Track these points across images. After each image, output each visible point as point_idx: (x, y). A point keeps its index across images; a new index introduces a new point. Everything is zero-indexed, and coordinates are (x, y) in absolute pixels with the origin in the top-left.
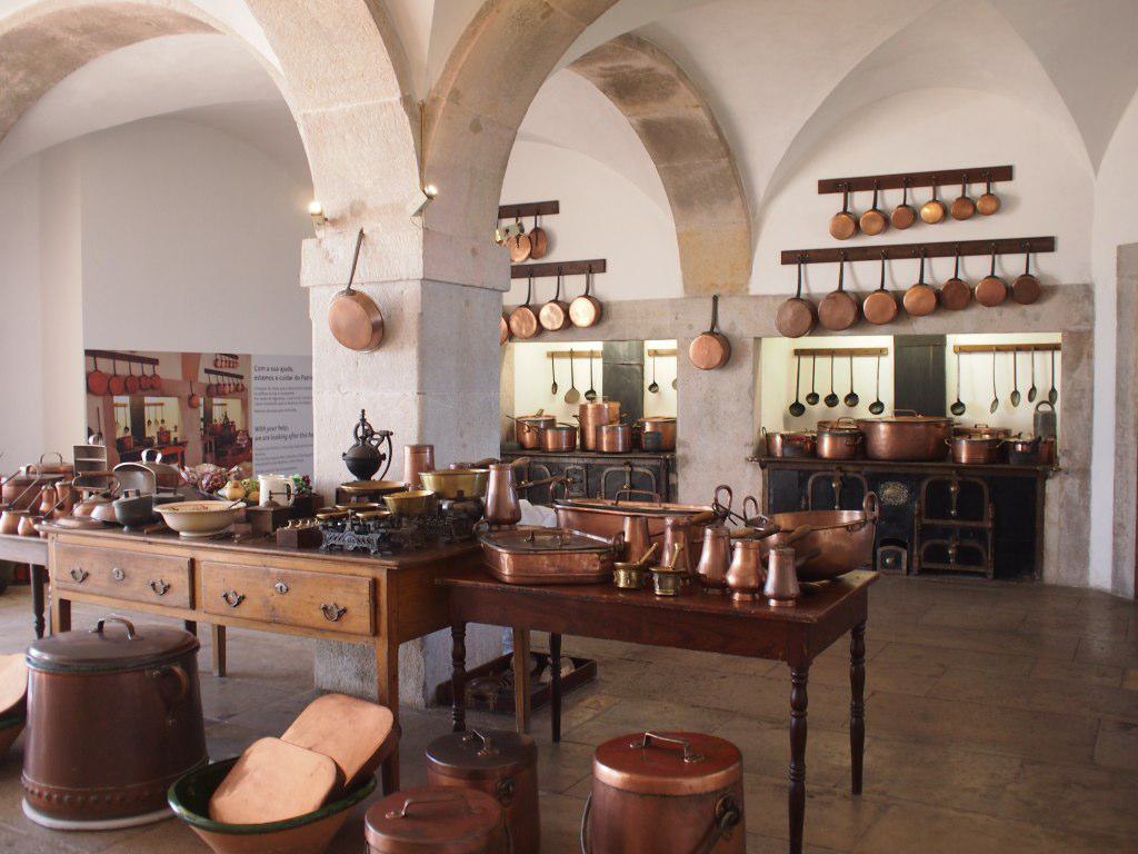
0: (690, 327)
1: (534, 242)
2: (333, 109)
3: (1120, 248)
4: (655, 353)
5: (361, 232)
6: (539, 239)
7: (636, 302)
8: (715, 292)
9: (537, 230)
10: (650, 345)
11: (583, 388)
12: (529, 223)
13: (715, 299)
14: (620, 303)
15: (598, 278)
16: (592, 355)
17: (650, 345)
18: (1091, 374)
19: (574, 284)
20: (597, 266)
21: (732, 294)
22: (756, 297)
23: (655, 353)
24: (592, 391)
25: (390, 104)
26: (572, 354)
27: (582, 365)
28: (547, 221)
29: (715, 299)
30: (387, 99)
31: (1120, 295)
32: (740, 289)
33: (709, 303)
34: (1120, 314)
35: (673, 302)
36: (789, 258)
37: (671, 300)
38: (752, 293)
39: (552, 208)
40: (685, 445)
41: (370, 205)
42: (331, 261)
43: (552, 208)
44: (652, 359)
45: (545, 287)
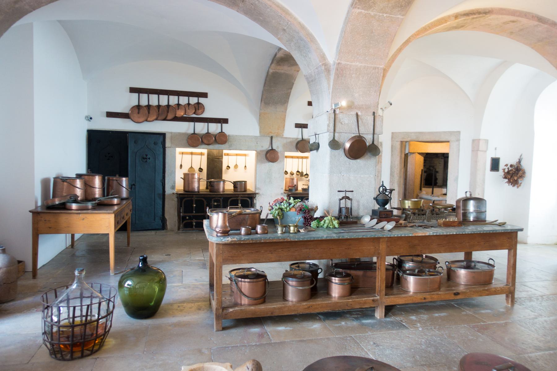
0: (262, 147)
1: (197, 107)
2: (353, 64)
3: (392, 133)
4: (228, 155)
5: (357, 115)
6: (199, 107)
7: (241, 136)
8: (271, 135)
9: (198, 103)
10: (225, 152)
11: (196, 168)
12: (194, 100)
13: (272, 138)
14: (233, 136)
15: (224, 125)
16: (202, 154)
17: (225, 152)
18: (381, 167)
19: (214, 128)
20: (225, 121)
21: (277, 136)
22: (286, 138)
23: (228, 155)
24: (200, 168)
25: (378, 68)
26: (192, 154)
27: (197, 158)
28: (202, 100)
29: (272, 138)
30: (378, 66)
31: (392, 146)
32: (280, 135)
33: (269, 139)
34: (392, 151)
35: (256, 137)
36: (298, 126)
37: (255, 136)
38: (284, 136)
39: (205, 95)
40: (259, 189)
41: (356, 104)
42: (342, 123)
43: (205, 95)
44: (227, 157)
45: (201, 128)
